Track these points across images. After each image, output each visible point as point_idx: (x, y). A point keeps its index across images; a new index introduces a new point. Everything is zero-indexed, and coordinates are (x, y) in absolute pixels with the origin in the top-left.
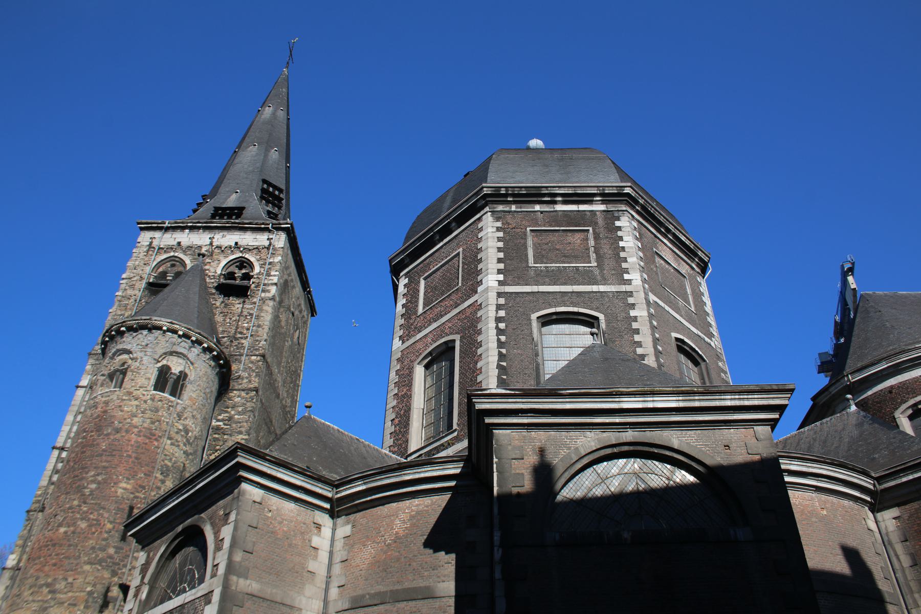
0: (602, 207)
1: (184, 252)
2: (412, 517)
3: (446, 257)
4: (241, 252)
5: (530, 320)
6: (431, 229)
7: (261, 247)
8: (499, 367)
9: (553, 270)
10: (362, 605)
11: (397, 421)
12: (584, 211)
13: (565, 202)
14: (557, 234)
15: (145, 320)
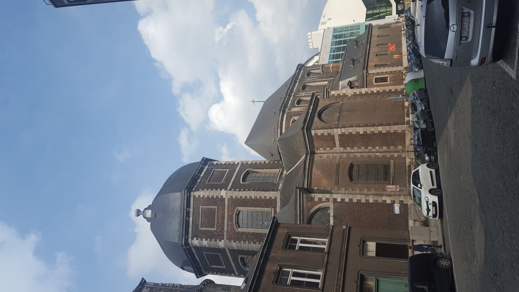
0: (207, 167)
2: (317, 169)
5: (243, 184)
6: (183, 219)
8: (257, 191)
10: (338, 181)
13: (201, 174)
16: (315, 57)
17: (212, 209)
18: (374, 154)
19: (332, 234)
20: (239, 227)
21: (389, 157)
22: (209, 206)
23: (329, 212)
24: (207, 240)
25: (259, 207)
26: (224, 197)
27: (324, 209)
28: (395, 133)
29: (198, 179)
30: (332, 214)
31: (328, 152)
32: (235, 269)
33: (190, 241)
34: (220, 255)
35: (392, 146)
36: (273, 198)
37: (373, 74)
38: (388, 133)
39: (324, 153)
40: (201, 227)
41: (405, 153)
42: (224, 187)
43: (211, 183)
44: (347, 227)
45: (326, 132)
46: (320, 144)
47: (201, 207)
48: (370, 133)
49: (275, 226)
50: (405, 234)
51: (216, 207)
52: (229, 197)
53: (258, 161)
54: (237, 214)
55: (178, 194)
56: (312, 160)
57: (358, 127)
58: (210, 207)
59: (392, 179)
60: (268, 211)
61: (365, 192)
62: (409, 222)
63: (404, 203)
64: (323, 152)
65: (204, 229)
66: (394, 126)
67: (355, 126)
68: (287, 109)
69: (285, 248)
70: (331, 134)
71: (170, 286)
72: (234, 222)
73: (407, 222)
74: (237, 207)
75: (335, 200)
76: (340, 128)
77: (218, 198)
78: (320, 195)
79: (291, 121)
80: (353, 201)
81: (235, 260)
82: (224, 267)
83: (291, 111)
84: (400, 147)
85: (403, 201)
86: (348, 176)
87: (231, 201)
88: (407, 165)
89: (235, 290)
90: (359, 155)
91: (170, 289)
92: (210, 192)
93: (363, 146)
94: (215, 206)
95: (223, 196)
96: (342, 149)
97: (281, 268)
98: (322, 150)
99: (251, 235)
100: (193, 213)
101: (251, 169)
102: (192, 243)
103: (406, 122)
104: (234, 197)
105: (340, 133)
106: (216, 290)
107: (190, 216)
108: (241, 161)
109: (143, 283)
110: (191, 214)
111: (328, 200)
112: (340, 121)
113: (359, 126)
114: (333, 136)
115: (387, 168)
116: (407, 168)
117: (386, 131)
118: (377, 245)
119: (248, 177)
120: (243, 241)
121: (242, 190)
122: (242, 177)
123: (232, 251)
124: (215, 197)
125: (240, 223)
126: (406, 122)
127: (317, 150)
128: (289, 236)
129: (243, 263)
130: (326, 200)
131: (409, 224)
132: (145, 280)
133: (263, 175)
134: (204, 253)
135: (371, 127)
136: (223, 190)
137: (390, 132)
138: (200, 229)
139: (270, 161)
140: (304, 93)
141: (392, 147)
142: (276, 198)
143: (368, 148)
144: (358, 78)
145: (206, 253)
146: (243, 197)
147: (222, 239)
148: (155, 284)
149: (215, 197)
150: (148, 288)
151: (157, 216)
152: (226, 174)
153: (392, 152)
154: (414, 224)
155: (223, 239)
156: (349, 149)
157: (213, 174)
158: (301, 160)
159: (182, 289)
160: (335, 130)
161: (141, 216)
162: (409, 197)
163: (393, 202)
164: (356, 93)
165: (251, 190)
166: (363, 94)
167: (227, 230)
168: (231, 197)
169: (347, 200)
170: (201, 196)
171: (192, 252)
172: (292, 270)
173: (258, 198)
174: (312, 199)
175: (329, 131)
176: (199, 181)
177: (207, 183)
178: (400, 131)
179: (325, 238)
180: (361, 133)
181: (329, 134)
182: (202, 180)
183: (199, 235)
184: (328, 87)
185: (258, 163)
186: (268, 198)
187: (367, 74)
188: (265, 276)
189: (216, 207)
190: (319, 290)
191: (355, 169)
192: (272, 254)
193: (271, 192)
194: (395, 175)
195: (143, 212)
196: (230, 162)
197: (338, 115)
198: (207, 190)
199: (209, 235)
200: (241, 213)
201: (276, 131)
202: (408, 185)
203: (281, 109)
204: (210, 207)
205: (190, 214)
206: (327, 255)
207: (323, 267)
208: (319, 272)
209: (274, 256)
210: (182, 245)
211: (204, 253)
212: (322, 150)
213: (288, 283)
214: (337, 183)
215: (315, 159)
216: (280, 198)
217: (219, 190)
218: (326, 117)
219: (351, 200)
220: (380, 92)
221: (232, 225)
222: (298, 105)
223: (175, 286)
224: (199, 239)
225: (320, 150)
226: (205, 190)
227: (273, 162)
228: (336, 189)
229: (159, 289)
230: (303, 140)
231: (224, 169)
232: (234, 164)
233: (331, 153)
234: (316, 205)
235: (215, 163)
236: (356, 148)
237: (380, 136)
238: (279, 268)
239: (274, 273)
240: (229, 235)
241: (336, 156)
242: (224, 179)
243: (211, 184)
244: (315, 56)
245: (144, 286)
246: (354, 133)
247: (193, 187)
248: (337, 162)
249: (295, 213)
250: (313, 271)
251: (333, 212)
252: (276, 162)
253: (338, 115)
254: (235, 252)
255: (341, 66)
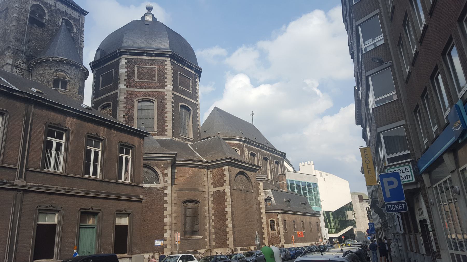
0: (193, 72)
1: (44, 5)
3: (149, 65)
4: (68, 17)
6: (145, 51)
7: (76, 19)
8: (172, 118)
9: (183, 90)
11: (126, 117)
12: (190, 72)
13: (187, 67)
14: (184, 77)
15: (76, 63)
16: (292, 168)
17: (155, 77)
18: (208, 222)
19: (135, 186)
20: (138, 102)
21: (205, 234)
22: (158, 75)
23: (155, 183)
24: (125, 72)
25: (158, 121)
26: (166, 88)
27: (158, 179)
28: (227, 239)
29: (182, 64)
30: (153, 185)
31: (209, 181)
32: (99, 98)
33: (124, 56)
34: (112, 84)
35: (215, 237)
36: (166, 133)
37: (278, 219)
38: (226, 233)
39: (208, 177)
40: (137, 67)
41: (209, 248)
42: (176, 88)
43: (179, 76)
44: (142, 199)
45: (227, 179)
46: (216, 174)
47: (157, 67)
48: (226, 217)
49: (141, 135)
50: (136, 251)
51: (156, 81)
52: (166, 93)
53: (200, 119)
54: (151, 100)
55: (167, 46)
56: (201, 167)
57: (231, 206)
58: (156, 75)
59: (186, 238)
60: (154, 128)
61: (173, 214)
62: (147, 254)
63: (164, 249)
64: (209, 176)
65: (136, 69)
66: (232, 238)
67: (232, 204)
68: (246, 144)
69: (120, 144)
70: (225, 183)
71: (82, 38)
72: (143, 98)
73: (147, 252)
74: (157, 100)
75: (165, 188)
76: (230, 191)
77: (165, 83)
78: (170, 175)
79: (236, 148)
80: (165, 204)
81: (107, 99)
82: (100, 89)
83: (245, 148)
84: (214, 244)
85: (166, 248)
86: (188, 199)
87: (162, 95)
88: (198, 250)
89: (80, 98)
90: (206, 208)
91: (79, 38)
92: (170, 75)
93: (214, 212)
94: (158, 80)
95: (167, 87)
96: (212, 193)
97: (102, 140)
98: (210, 175)
99: (131, 113)
100: (151, 59)
101: (192, 113)
102: (123, 59)
103: (237, 248)
104: (166, 97)
105: (226, 191)
106: (79, 81)
107: (148, 57)
108: (199, 103)
109: (84, 13)
110: (149, 58)
111: (166, 182)
112: (236, 191)
113: (232, 208)
114: (223, 185)
115: (196, 233)
116: (196, 250)
117: (228, 231)
118: (126, 226)
119: (185, 110)
120: (125, 106)
121: (173, 105)
122: (185, 104)
123: (116, 96)
124: (166, 80)
125: (142, 103)
126: (237, 248)
127: (210, 172)
128: (132, 148)
129: (105, 106)
130: (165, 180)
131: (146, 254)
132: (86, 14)
133: (187, 123)
134: (114, 69)
135: (231, 218)
136: (173, 87)
137: (227, 235)
138: (136, 66)
139: (199, 130)
140: (261, 159)
141: (214, 237)
142: (166, 135)
143: (213, 215)
144: (274, 205)
145: (113, 71)
146: (166, 106)
147: (127, 86)
148: (83, 24)
149: (166, 80)
150: (79, 18)
151: (147, 26)
152: (187, 90)
153: (210, 237)
154: (145, 258)
155: (127, 87)
156: (212, 199)
157: (187, 78)
158: (201, 157)
159: (79, 50)
160: (229, 187)
161: (146, 11)
162: (170, 253)
163: (165, 240)
164: (261, 204)
165: (173, 113)
166: (260, 211)
167: (136, 91)
168: (166, 95)
169: (166, 199)
170: (166, 67)
171: (114, 59)
172: (100, 151)
173: (166, 119)
174: (166, 168)
175: (228, 182)
176: (181, 65)
177: (179, 72)
178: (228, 243)
179: (131, 180)
180: (226, 210)
181: (225, 182)
182: (181, 68)
183: (130, 65)
184: (266, 180)
185: (198, 119)
186: (166, 128)
187: (278, 213)
188: (94, 126)
189: (157, 81)
190: (83, 175)
191: (194, 205)
192: (114, 133)
193: (172, 131)
194: (189, 241)
195: (150, 13)
196: (198, 94)
197: (242, 189)
198: (173, 73)
199: (130, 74)
200: (152, 104)
201: (227, 135)
202: (181, 251)
203: (247, 139)
204: (156, 75)
205: (149, 57)
206: (115, 182)
207: (104, 178)
208: (100, 175)
209: (113, 134)
210: (120, 49)
211: (114, 69)
212: (210, 176)
213: (88, 147)
214: (181, 190)
215: (202, 170)
216: (167, 139)
217: (173, 83)
218: (240, 178)
219: (166, 202)
220: (262, 225)
221: (140, 96)
222: (250, 154)
223: (82, 43)
224: (126, 66)
225: (211, 174)
226: (172, 71)
227: (199, 132)
228: (176, 189)
229: (79, 28)
230: (219, 158)
231: (191, 88)
232: (197, 97)
233: (208, 183)
234: (161, 171)
235: (197, 80)
236: (213, 205)
237: (224, 226)
238: (102, 139)
239: (97, 134)
240: (130, 93)
241: (205, 188)
242: (183, 88)
243: (178, 76)
244: (293, 168)
245: (80, 14)
246: (226, 203)
247: (174, 60)
248: (200, 189)
249: (152, 153)
250: (100, 169)
251: (154, 186)
252: (199, 135)
253: (241, 189)
254: (115, 98)
255: (284, 191)
